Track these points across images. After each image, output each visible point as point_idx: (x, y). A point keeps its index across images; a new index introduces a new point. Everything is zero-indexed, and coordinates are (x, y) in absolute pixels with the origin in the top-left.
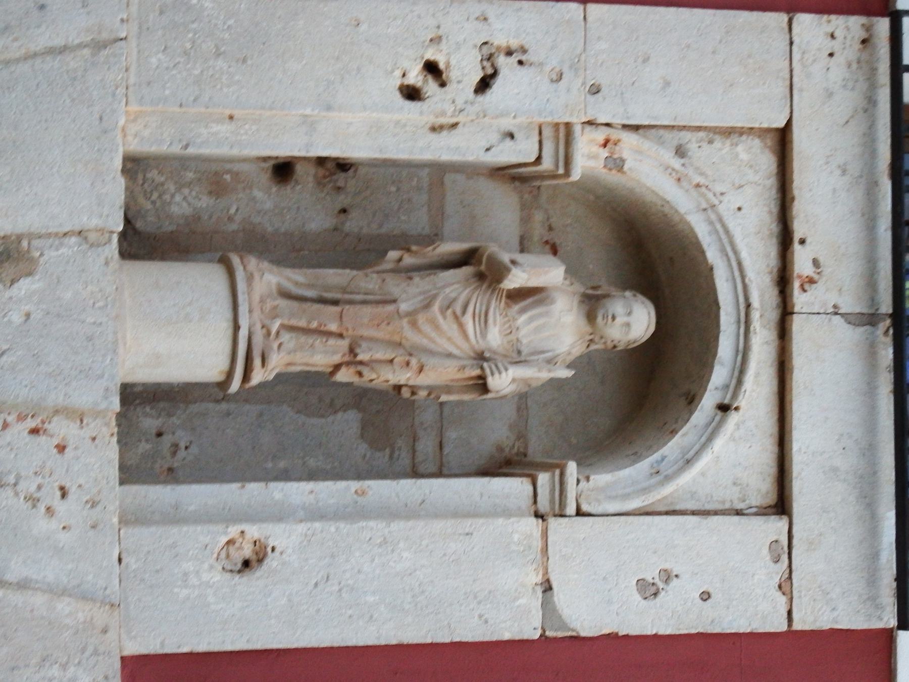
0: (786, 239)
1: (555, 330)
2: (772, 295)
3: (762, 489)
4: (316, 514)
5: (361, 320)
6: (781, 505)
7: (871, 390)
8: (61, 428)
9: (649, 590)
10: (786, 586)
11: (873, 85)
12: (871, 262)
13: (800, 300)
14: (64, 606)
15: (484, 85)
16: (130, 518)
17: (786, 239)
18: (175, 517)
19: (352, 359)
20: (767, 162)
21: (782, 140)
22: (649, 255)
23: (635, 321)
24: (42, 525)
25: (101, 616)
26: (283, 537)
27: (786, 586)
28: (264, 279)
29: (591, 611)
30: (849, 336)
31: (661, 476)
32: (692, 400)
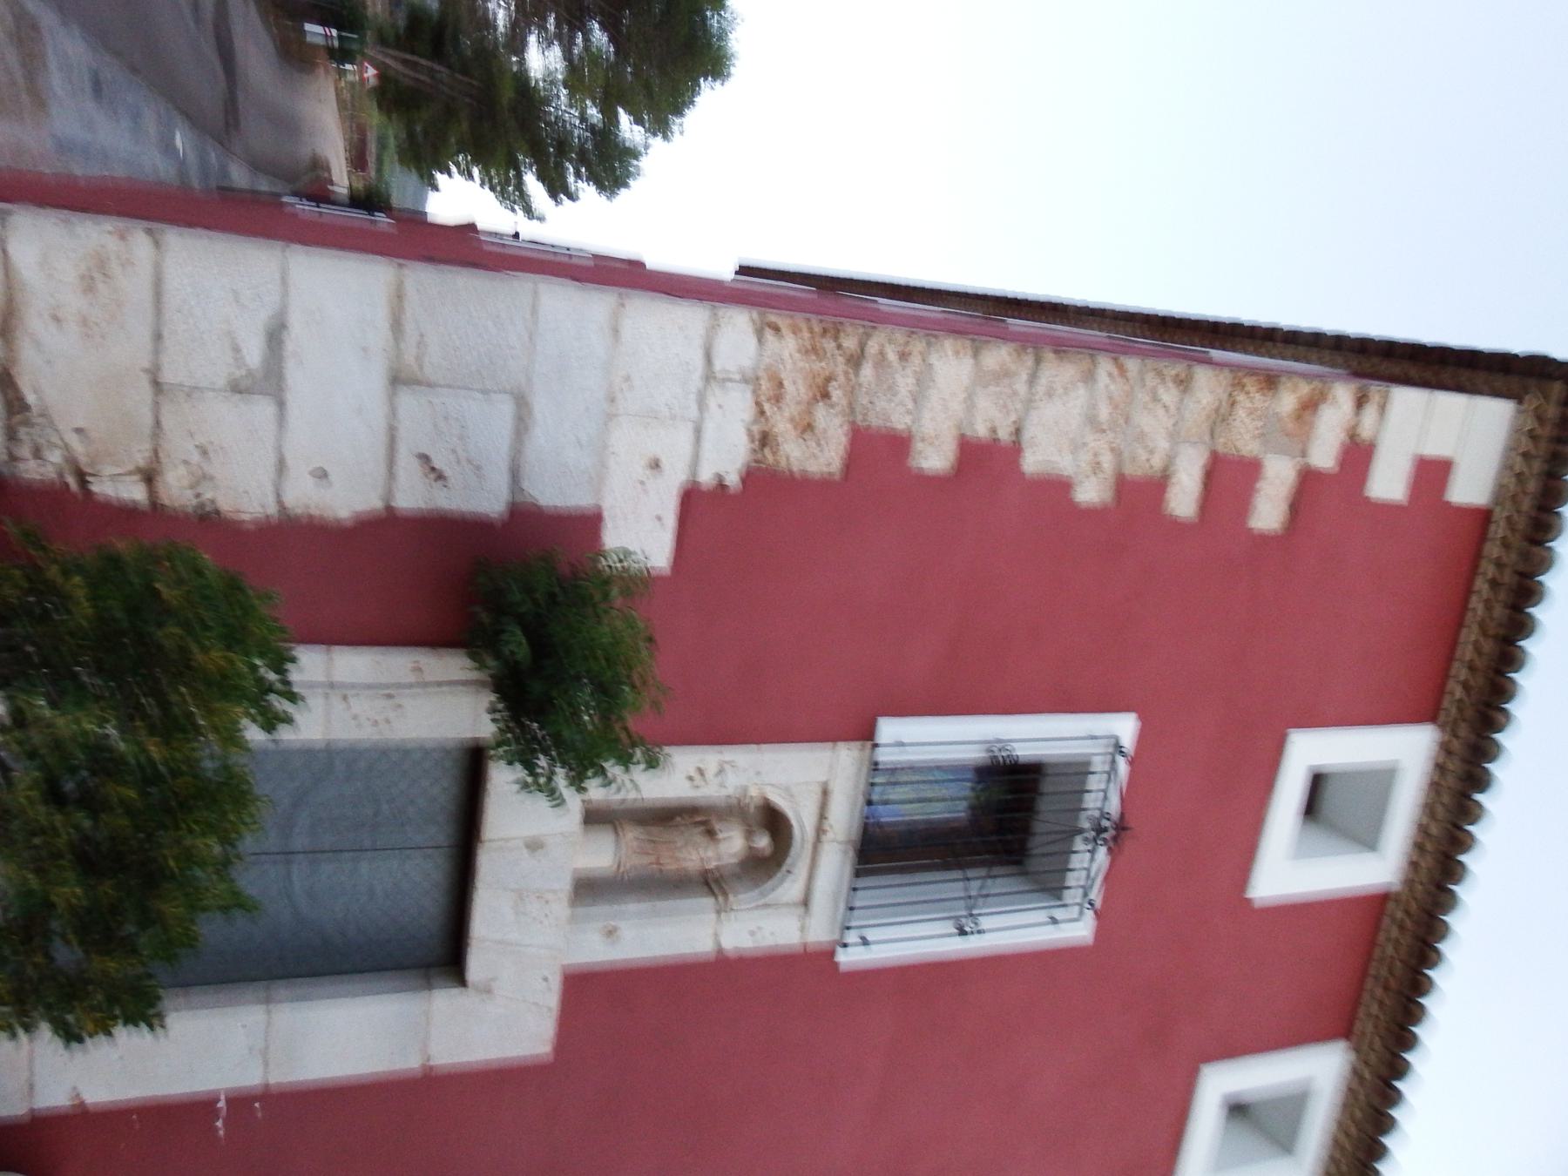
1: (732, 844)
8: (550, 896)
23: (763, 842)
28: (632, 834)
31: (763, 895)
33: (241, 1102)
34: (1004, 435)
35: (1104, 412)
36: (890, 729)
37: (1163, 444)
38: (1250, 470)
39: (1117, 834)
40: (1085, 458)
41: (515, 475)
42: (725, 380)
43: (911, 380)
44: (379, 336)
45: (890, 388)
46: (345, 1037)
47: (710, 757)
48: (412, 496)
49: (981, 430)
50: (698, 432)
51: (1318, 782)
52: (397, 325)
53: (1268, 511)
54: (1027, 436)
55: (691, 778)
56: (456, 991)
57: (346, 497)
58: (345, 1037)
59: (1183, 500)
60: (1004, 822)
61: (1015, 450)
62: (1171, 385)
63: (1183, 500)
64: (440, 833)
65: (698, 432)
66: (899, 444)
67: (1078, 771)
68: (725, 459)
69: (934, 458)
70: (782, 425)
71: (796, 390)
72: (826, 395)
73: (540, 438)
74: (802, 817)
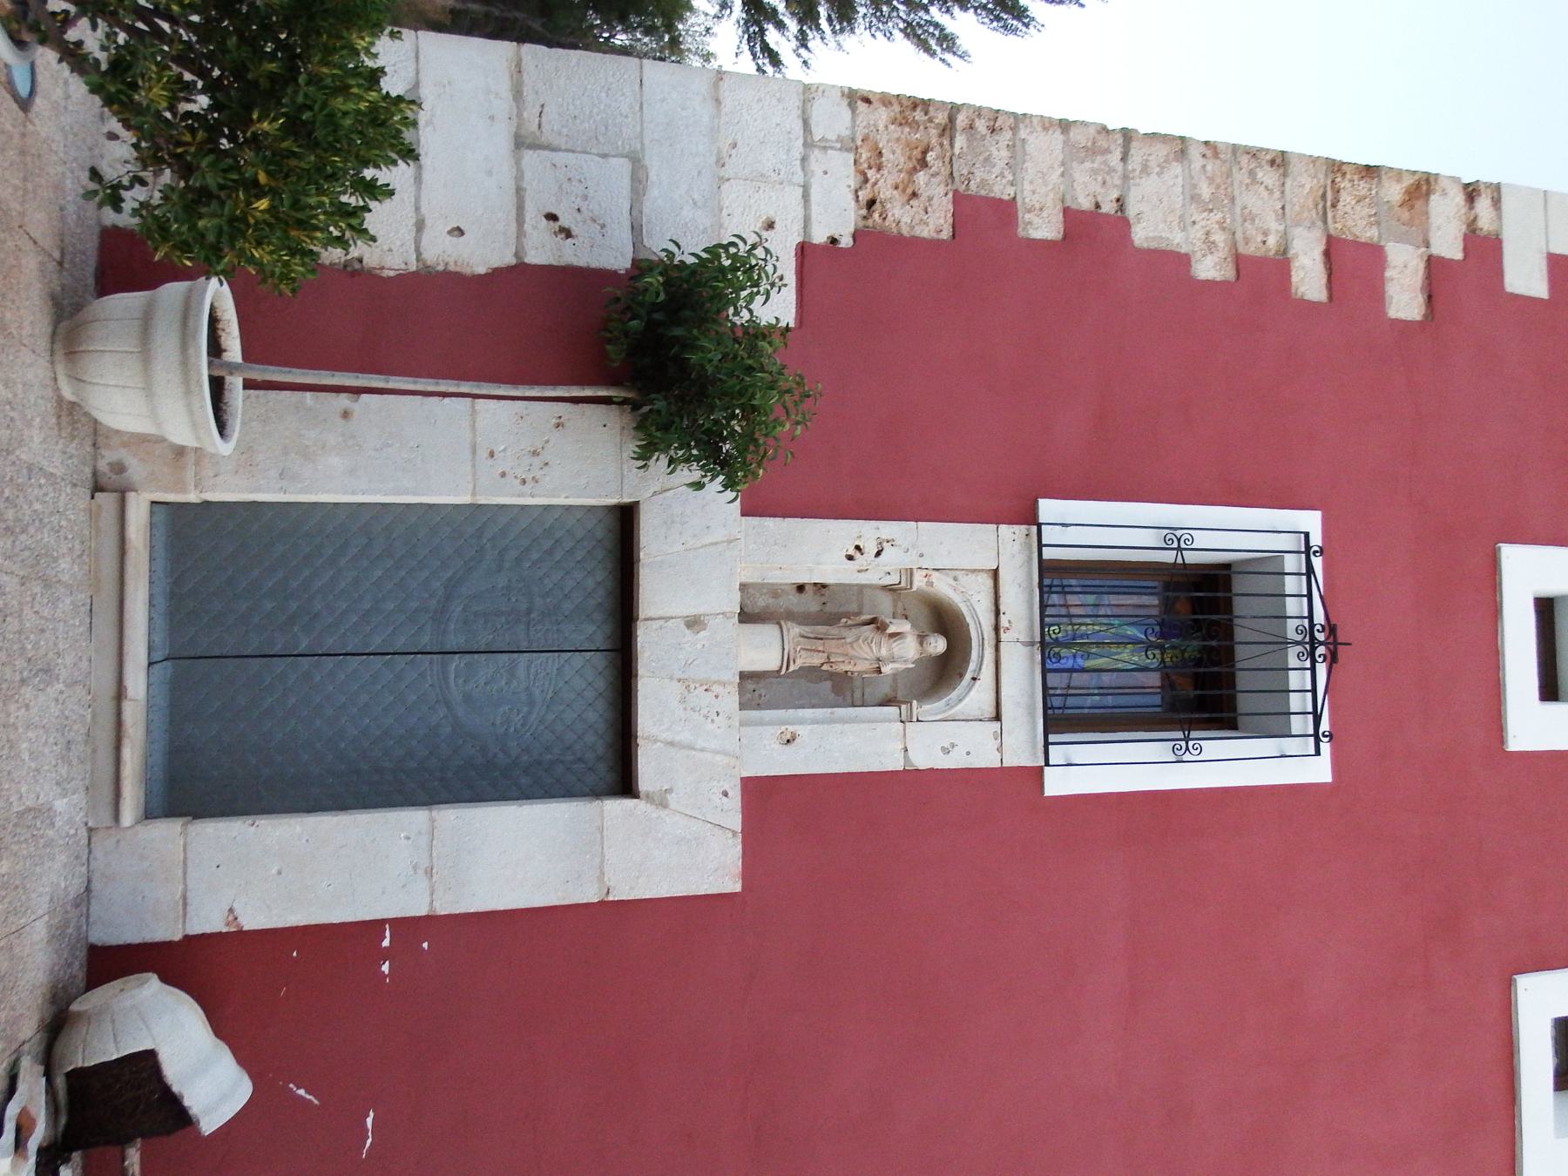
0: (997, 613)
1: (907, 649)
2: (993, 634)
3: (990, 711)
4: (815, 722)
5: (832, 646)
6: (998, 717)
7: (1033, 671)
8: (716, 689)
9: (946, 751)
10: (1000, 749)
11: (1031, 552)
12: (1031, 621)
13: (1003, 636)
14: (718, 758)
15: (878, 554)
16: (742, 724)
17: (997, 613)
18: (761, 723)
19: (829, 662)
20: (990, 582)
21: (995, 574)
23: (938, 645)
24: (710, 726)
25: (733, 762)
26: (801, 730)
27: (1000, 749)
28: (794, 630)
29: (922, 761)
30: (1024, 650)
31: (950, 706)
32: (961, 676)
33: (406, 927)
34: (1108, 208)
35: (1205, 191)
36: (1049, 509)
37: (1275, 226)
38: (1374, 255)
39: (1329, 643)
40: (1197, 234)
41: (636, 229)
42: (825, 148)
43: (1005, 153)
44: (503, 104)
45: (987, 160)
46: (512, 857)
47: (869, 531)
48: (542, 250)
49: (1085, 204)
50: (806, 196)
51: (1546, 608)
52: (518, 94)
53: (1404, 299)
54: (1131, 212)
55: (850, 558)
56: (628, 803)
57: (482, 253)
58: (512, 857)
59: (1309, 279)
60: (1195, 642)
61: (1121, 223)
62: (1267, 168)
63: (1309, 279)
64: (596, 631)
65: (806, 196)
66: (1006, 211)
67: (1268, 567)
68: (836, 220)
69: (1043, 226)
70: (885, 192)
71: (894, 157)
72: (923, 163)
73: (654, 197)
74: (973, 604)
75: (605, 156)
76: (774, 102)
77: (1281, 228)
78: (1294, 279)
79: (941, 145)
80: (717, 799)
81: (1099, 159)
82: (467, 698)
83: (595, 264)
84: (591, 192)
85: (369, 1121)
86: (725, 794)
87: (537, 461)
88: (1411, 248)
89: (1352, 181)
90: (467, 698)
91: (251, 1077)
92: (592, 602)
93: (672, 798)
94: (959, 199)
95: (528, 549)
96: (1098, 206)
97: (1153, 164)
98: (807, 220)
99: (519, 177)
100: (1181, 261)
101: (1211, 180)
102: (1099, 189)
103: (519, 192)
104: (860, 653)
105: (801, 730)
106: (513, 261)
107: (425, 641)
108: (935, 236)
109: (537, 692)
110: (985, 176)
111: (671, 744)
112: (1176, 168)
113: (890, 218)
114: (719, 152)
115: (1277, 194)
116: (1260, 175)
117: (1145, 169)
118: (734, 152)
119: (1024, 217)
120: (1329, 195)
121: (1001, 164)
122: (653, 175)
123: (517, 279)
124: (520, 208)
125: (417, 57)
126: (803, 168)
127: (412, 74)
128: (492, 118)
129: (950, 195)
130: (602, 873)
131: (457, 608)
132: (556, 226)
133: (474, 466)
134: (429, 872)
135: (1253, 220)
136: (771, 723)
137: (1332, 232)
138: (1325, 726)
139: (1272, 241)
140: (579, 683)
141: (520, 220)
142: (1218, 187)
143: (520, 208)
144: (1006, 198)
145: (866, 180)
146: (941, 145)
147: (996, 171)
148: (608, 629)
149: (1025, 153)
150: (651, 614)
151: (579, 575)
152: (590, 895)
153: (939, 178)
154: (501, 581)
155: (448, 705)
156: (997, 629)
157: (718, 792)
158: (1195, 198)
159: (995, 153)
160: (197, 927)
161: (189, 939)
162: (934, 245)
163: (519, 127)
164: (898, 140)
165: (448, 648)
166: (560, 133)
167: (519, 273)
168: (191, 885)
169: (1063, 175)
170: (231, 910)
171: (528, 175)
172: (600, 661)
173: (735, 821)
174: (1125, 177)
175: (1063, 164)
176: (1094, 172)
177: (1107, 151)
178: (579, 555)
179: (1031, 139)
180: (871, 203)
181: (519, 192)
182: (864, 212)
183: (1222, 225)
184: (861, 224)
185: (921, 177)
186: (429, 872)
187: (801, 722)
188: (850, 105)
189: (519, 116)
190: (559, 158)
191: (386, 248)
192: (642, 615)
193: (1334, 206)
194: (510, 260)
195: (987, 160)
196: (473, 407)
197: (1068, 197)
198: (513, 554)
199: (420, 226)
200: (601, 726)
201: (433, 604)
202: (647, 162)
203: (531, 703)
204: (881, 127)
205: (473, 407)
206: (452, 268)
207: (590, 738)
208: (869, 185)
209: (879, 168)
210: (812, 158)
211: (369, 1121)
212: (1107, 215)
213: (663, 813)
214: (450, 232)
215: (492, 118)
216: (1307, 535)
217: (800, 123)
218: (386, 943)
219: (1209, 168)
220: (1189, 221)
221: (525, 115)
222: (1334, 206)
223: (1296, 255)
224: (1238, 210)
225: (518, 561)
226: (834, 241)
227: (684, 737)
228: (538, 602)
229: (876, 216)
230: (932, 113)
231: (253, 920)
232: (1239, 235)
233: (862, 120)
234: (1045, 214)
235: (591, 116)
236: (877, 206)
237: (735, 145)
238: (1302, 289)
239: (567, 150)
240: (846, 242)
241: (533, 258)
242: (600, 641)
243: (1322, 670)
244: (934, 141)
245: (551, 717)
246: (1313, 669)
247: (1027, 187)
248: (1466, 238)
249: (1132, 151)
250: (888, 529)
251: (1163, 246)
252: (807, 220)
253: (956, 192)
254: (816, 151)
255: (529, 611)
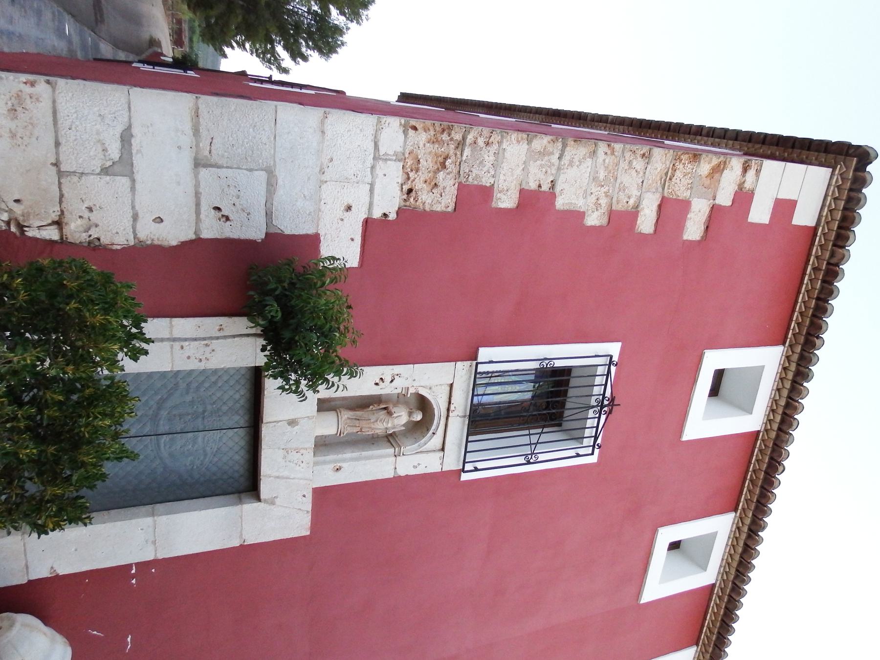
0: (450, 403)
1: (401, 418)
2: (446, 412)
3: (440, 446)
4: (352, 459)
5: (364, 424)
6: (443, 449)
7: (463, 429)
8: (302, 451)
9: (415, 467)
10: (442, 464)
11: (470, 377)
12: (468, 389)
13: (451, 414)
14: (301, 481)
15: (392, 381)
16: (316, 464)
17: (450, 403)
18: (325, 463)
19: (361, 431)
20: (448, 388)
21: (451, 385)
22: (423, 404)
23: (418, 417)
24: (298, 468)
25: (309, 482)
26: (344, 465)
27: (442, 464)
28: (346, 415)
29: (402, 472)
30: (460, 420)
32: (428, 430)
33: (143, 566)
34: (545, 188)
35: (602, 175)
36: (484, 353)
37: (635, 193)
38: (685, 206)
40: (592, 199)
41: (269, 215)
42: (386, 160)
43: (492, 158)
44: (187, 139)
45: (481, 163)
46: (197, 530)
47: (387, 371)
48: (211, 230)
49: (533, 186)
50: (372, 191)
52: (196, 132)
53: (693, 230)
54: (558, 189)
55: (377, 384)
57: (173, 233)
58: (197, 530)
59: (646, 223)
60: (550, 401)
61: (552, 195)
62: (640, 159)
63: (646, 223)
64: (241, 419)
65: (372, 191)
66: (487, 192)
67: (589, 372)
68: (388, 203)
69: (506, 201)
70: (419, 185)
71: (427, 163)
72: (443, 166)
73: (281, 194)
74: (439, 402)
75: (251, 170)
76: (358, 131)
77: (639, 194)
78: (638, 222)
79: (456, 155)
80: (300, 499)
81: (546, 158)
82: (171, 455)
83: (243, 237)
84: (242, 194)
85: (129, 639)
86: (304, 496)
87: (208, 349)
88: (705, 201)
89: (684, 164)
90: (171, 455)
91: (71, 645)
92: (238, 405)
93: (277, 501)
94: (462, 188)
95: (203, 382)
96: (540, 186)
97: (576, 160)
98: (371, 205)
99: (197, 186)
100: (580, 215)
101: (606, 168)
102: (542, 177)
103: (197, 195)
104: (381, 425)
105: (344, 465)
106: (193, 237)
107: (147, 430)
108: (444, 209)
109: (208, 449)
110: (478, 172)
111: (278, 477)
112: (589, 162)
113: (420, 201)
114: (322, 164)
115: (642, 173)
116: (634, 163)
117: (571, 164)
118: (330, 164)
119: (497, 195)
120: (669, 174)
121: (488, 165)
122: (280, 182)
123: (195, 246)
124: (198, 205)
125: (129, 108)
126: (372, 174)
127: (126, 120)
128: (179, 147)
129: (456, 186)
130: (241, 534)
131: (164, 413)
132: (220, 214)
133: (172, 354)
134: (154, 542)
135: (624, 190)
136: (330, 462)
137: (666, 195)
138: (599, 441)
139: (632, 202)
140: (231, 444)
141: (198, 212)
142: (610, 172)
143: (198, 205)
144: (488, 185)
145: (408, 178)
146: (456, 155)
147: (485, 169)
148: (247, 417)
149: (504, 157)
150: (269, 420)
151: (231, 393)
152: (236, 543)
153: (451, 175)
154: (188, 398)
155: (161, 459)
156: (448, 410)
157: (300, 494)
158: (595, 179)
159: (486, 158)
160: (33, 577)
161: (30, 582)
162: (443, 215)
163: (197, 153)
164: (430, 153)
165: (160, 432)
166: (223, 156)
167: (196, 245)
168: (29, 560)
169: (523, 170)
170: (52, 568)
171: (203, 184)
172: (242, 432)
173: (309, 507)
174: (559, 169)
175: (525, 163)
176: (542, 166)
177: (552, 153)
178: (232, 382)
179: (509, 149)
180: (410, 191)
181: (197, 195)
182: (405, 197)
183: (606, 194)
184: (403, 203)
185: (441, 175)
186: (154, 542)
187: (344, 460)
188: (404, 132)
189: (197, 145)
190: (223, 172)
191: (115, 231)
192: (264, 421)
193: (670, 179)
194: (191, 236)
195: (481, 163)
196: (171, 323)
197: (524, 183)
198: (194, 385)
199: (135, 217)
200: (242, 462)
201: (151, 412)
202: (277, 173)
203: (206, 455)
204: (421, 146)
205: (171, 323)
206: (156, 242)
207: (237, 468)
208: (409, 182)
209: (417, 170)
210: (378, 167)
211: (129, 639)
212: (544, 192)
213: (272, 507)
214: (154, 220)
215: (179, 147)
216: (611, 357)
217: (373, 144)
218: (133, 571)
219: (607, 161)
220: (589, 193)
221: (201, 145)
222: (670, 179)
223: (643, 209)
224: (617, 185)
225: (198, 388)
226: (385, 215)
227: (286, 473)
228: (209, 407)
229: (412, 199)
230: (453, 135)
231: (63, 571)
232: (614, 200)
233: (410, 142)
234: (509, 194)
235: (242, 145)
236: (413, 194)
237: (331, 160)
238: (641, 227)
239: (227, 167)
240: (392, 216)
241: (206, 235)
242: (242, 423)
243: (603, 417)
244: (452, 153)
245: (216, 459)
246: (599, 418)
247: (502, 177)
248: (736, 193)
249: (566, 153)
250: (397, 369)
251: (572, 208)
252: (371, 205)
253: (460, 183)
254: (381, 162)
255: (204, 412)
